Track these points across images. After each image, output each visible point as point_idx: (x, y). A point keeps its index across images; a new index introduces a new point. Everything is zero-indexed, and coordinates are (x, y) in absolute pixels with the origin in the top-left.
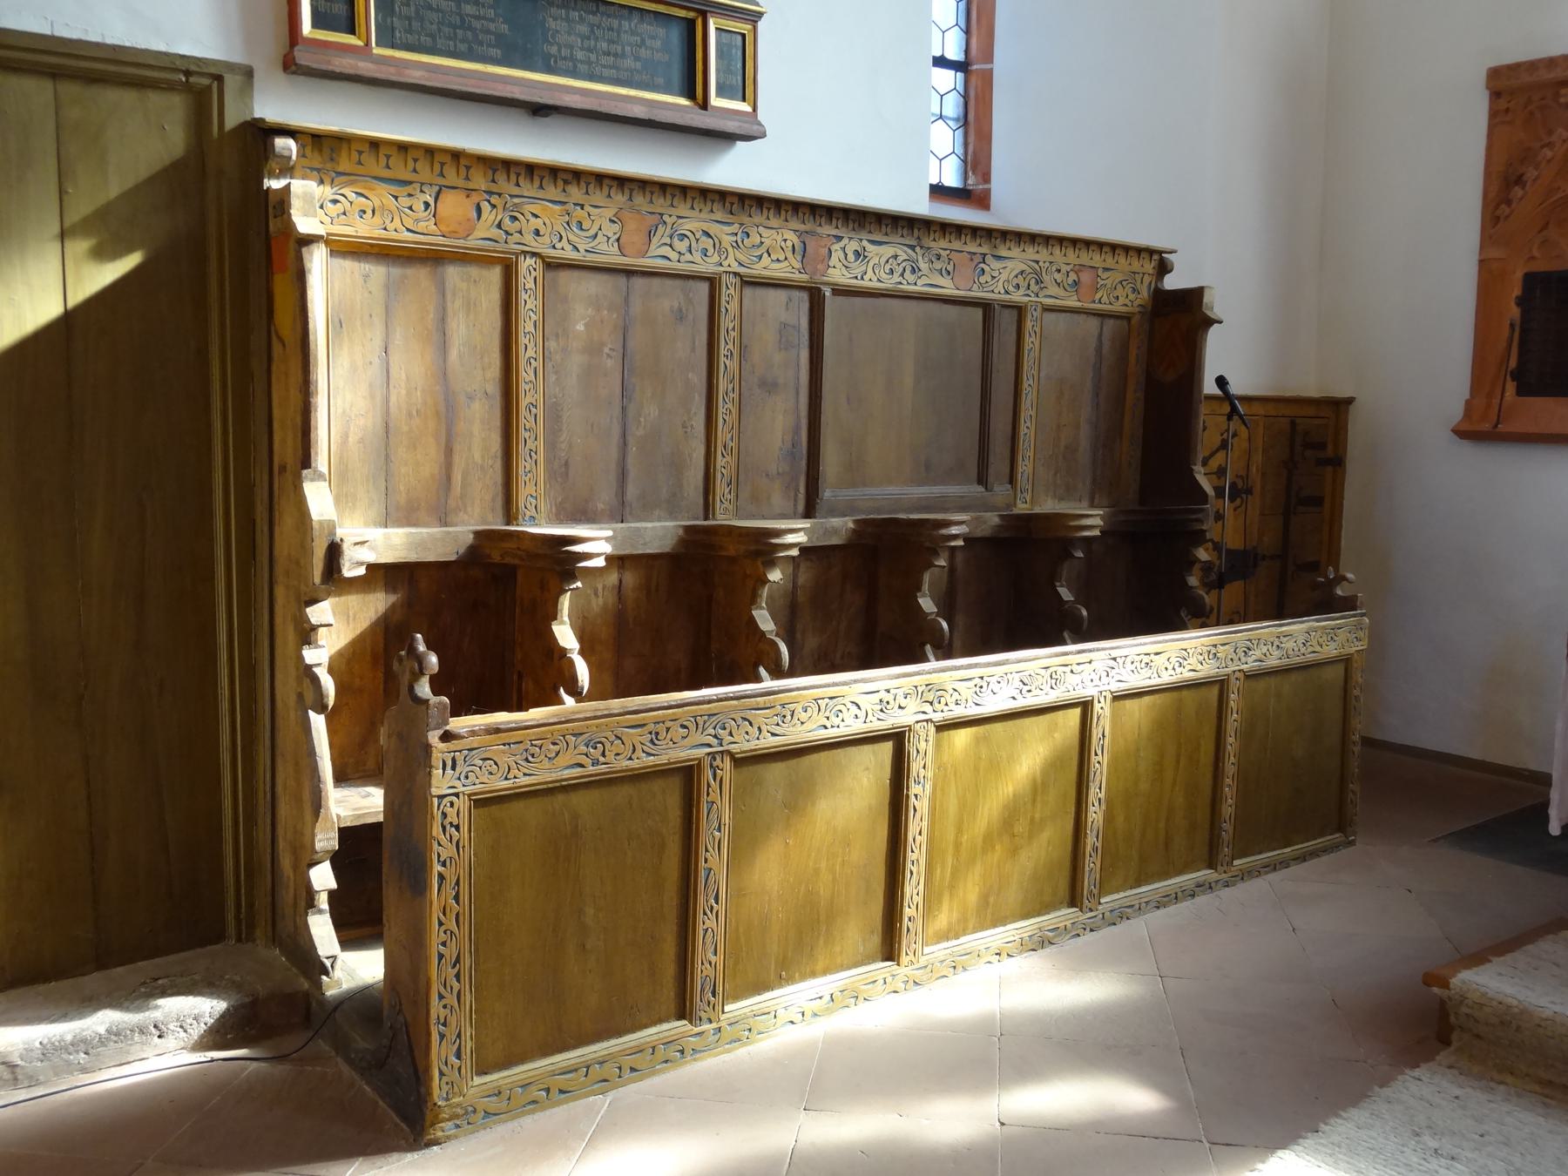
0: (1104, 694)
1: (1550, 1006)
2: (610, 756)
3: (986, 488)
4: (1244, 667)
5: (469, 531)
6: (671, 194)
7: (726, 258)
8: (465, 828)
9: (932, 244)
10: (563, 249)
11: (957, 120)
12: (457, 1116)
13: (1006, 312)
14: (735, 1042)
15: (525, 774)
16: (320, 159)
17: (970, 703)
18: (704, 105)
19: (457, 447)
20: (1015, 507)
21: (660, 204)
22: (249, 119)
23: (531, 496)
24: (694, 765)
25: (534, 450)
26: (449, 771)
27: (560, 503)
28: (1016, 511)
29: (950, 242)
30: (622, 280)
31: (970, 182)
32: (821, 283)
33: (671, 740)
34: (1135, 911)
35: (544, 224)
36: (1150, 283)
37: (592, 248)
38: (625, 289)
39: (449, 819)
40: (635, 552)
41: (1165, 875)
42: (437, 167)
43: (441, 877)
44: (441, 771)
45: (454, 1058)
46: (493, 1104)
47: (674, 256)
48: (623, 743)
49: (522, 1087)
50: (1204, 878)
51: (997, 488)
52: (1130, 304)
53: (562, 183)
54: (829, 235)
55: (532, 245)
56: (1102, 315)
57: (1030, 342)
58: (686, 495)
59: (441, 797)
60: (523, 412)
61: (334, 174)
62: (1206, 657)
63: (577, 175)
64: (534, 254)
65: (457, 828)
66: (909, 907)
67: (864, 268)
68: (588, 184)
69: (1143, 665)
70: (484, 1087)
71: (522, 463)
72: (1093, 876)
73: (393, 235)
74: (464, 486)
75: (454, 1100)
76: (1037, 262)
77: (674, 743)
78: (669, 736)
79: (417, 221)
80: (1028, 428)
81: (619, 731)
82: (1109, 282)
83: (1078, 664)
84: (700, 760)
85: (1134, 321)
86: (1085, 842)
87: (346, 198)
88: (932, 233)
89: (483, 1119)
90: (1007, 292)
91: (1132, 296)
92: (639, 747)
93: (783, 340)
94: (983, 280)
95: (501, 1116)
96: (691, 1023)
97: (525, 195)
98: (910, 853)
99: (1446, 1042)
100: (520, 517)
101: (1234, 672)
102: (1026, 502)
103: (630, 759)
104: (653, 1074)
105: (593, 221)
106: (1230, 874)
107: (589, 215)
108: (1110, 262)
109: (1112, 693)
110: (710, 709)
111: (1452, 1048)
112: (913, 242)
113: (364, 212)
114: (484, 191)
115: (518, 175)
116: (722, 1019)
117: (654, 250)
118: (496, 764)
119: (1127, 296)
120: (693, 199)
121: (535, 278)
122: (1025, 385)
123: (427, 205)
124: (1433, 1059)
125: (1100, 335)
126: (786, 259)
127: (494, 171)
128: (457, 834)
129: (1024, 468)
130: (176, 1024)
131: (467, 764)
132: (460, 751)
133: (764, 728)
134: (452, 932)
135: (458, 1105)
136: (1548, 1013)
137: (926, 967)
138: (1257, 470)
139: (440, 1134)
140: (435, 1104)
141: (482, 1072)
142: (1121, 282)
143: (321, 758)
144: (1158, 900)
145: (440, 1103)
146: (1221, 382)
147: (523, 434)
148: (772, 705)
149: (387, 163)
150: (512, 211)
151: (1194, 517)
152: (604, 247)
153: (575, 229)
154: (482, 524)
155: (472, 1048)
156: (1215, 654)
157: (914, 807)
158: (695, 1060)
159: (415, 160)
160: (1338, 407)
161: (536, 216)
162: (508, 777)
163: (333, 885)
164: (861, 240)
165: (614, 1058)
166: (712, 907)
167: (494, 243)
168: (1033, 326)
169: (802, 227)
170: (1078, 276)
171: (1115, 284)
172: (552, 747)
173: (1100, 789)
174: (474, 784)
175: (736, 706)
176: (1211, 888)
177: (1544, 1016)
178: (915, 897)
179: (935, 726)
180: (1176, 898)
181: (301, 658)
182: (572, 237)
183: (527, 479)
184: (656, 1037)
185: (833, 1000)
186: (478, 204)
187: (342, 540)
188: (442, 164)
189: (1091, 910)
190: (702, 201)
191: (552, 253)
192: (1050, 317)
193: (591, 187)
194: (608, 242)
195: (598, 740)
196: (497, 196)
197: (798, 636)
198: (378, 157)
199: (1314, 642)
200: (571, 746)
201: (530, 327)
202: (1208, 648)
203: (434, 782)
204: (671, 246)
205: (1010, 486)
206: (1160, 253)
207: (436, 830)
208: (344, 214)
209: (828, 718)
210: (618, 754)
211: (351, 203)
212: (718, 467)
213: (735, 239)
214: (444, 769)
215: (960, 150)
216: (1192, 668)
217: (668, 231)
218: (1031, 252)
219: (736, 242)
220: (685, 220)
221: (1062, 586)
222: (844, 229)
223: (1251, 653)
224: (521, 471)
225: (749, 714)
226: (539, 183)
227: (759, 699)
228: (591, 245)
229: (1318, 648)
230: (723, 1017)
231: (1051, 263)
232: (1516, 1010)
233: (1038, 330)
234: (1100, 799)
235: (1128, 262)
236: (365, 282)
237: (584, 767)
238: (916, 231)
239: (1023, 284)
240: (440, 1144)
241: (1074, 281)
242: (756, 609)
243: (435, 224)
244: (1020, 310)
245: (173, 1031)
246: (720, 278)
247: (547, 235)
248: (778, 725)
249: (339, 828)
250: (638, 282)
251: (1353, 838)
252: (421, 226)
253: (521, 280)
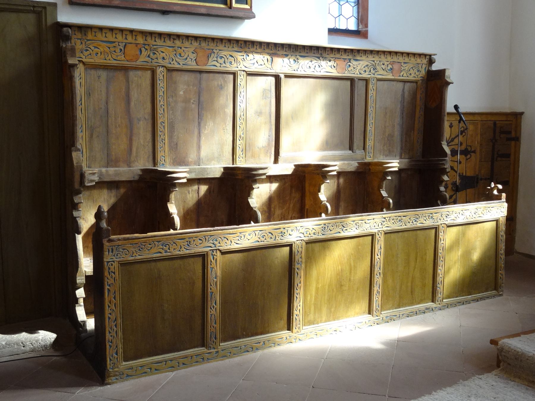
0: (380, 231)
1: (532, 352)
2: (172, 250)
3: (353, 152)
4: (446, 222)
5: (138, 169)
6: (216, 42)
7: (240, 65)
8: (117, 273)
9: (327, 56)
10: (174, 64)
11: (355, 2)
12: (116, 375)
13: (361, 82)
14: (224, 357)
15: (139, 255)
16: (81, 35)
17: (320, 234)
18: (231, 7)
19: (134, 138)
20: (366, 159)
21: (212, 45)
22: (55, 22)
23: (163, 156)
24: (205, 254)
25: (164, 139)
26: (111, 253)
27: (174, 159)
28: (366, 161)
29: (335, 54)
30: (198, 75)
31: (360, 27)
32: (280, 73)
33: (196, 245)
34: (397, 318)
35: (166, 55)
36: (426, 67)
37: (185, 63)
38: (199, 78)
39: (111, 270)
40: (203, 177)
41: (412, 304)
42: (124, 36)
43: (109, 290)
44: (107, 253)
45: (115, 355)
46: (130, 372)
47: (218, 65)
48: (177, 245)
49: (141, 367)
50: (429, 306)
51: (358, 152)
52: (416, 76)
53: (173, 40)
54: (282, 54)
55: (162, 63)
56: (404, 82)
57: (371, 93)
58: (224, 155)
59: (108, 262)
60: (159, 125)
61: (86, 40)
62: (428, 218)
63: (178, 36)
64: (163, 66)
65: (114, 273)
66: (296, 311)
67: (298, 66)
68: (183, 39)
69: (398, 221)
70: (127, 366)
71: (159, 144)
72: (377, 303)
73: (109, 62)
74: (137, 153)
75: (115, 369)
76: (374, 61)
77: (197, 246)
78: (194, 243)
79: (117, 56)
80: (371, 127)
81: (175, 241)
82: (407, 68)
83: (368, 220)
84: (207, 252)
85: (418, 83)
86: (373, 289)
87: (91, 49)
88: (327, 51)
89: (126, 377)
90: (360, 74)
91: (417, 73)
92: (183, 246)
93: (264, 95)
94: (349, 69)
95: (133, 376)
96: (206, 348)
97: (158, 44)
98: (296, 290)
99: (498, 366)
100: (158, 164)
101: (441, 224)
102: (371, 157)
103: (180, 251)
104: (191, 366)
105: (185, 53)
106: (442, 305)
107: (184, 51)
108: (407, 60)
109: (384, 231)
110: (210, 233)
111: (500, 369)
112: (319, 56)
113: (98, 54)
114: (143, 44)
115: (155, 37)
116: (219, 348)
117: (210, 63)
118: (128, 251)
119: (415, 73)
120: (225, 43)
121: (163, 75)
122: (369, 110)
123: (121, 50)
124: (491, 372)
125: (404, 89)
126: (264, 64)
127: (146, 36)
128: (114, 275)
129: (370, 143)
130: (29, 343)
131: (117, 251)
132: (115, 246)
133: (233, 241)
134: (113, 310)
135: (116, 371)
136: (531, 354)
137: (304, 334)
138: (478, 143)
139: (110, 381)
140: (109, 370)
141: (126, 360)
142: (412, 68)
143: (79, 250)
144: (408, 313)
145: (110, 370)
146: (456, 107)
147: (159, 133)
148: (236, 233)
149: (106, 35)
150: (154, 51)
151: (441, 163)
152: (190, 63)
153: (178, 56)
154: (143, 167)
155: (122, 352)
156: (432, 217)
157: (297, 272)
158: (208, 362)
159: (116, 34)
160: (517, 116)
161: (163, 52)
162: (133, 256)
163: (84, 296)
164: (296, 56)
165: (176, 359)
166: (214, 306)
167: (147, 63)
168: (373, 87)
169: (271, 52)
170: (393, 67)
171: (409, 69)
172: (149, 246)
173: (380, 269)
174: (120, 258)
175: (221, 233)
176: (433, 310)
177: (530, 355)
178: (298, 307)
179: (305, 242)
180: (416, 313)
181: (73, 215)
182: (177, 60)
183: (161, 150)
184: (192, 353)
185: (265, 344)
187: (85, 172)
188: (126, 35)
189: (377, 316)
190: (229, 43)
191: (170, 66)
192: (380, 83)
193: (184, 40)
194: (191, 60)
195: (167, 244)
196: (147, 46)
197: (272, 209)
198: (102, 33)
199: (480, 213)
200: (157, 245)
201: (161, 94)
202: (429, 215)
203: (105, 256)
204: (217, 61)
205: (363, 151)
206: (430, 56)
207: (106, 274)
208: (90, 54)
209: (259, 238)
210: (174, 249)
211: (93, 50)
212: (237, 145)
213: (243, 57)
214: (109, 252)
215: (356, 15)
216: (420, 222)
217: (216, 55)
218: (371, 57)
219: (244, 58)
220: (222, 51)
221: (383, 190)
222: (289, 52)
223: (449, 217)
224: (159, 147)
225: (227, 236)
226: (163, 40)
227: (230, 230)
228: (185, 62)
229: (481, 215)
230: (219, 347)
231: (380, 61)
232: (520, 353)
233: (375, 88)
234: (380, 273)
235: (415, 60)
236: (99, 79)
237: (162, 253)
238: (320, 51)
239: (368, 70)
240: (111, 384)
241: (391, 68)
242: (250, 198)
243: (124, 57)
244: (366, 81)
245: (28, 345)
246: (237, 72)
247: (167, 59)
248: (239, 240)
249: (85, 275)
250: (205, 76)
251: (502, 293)
252: (119, 58)
253: (158, 76)
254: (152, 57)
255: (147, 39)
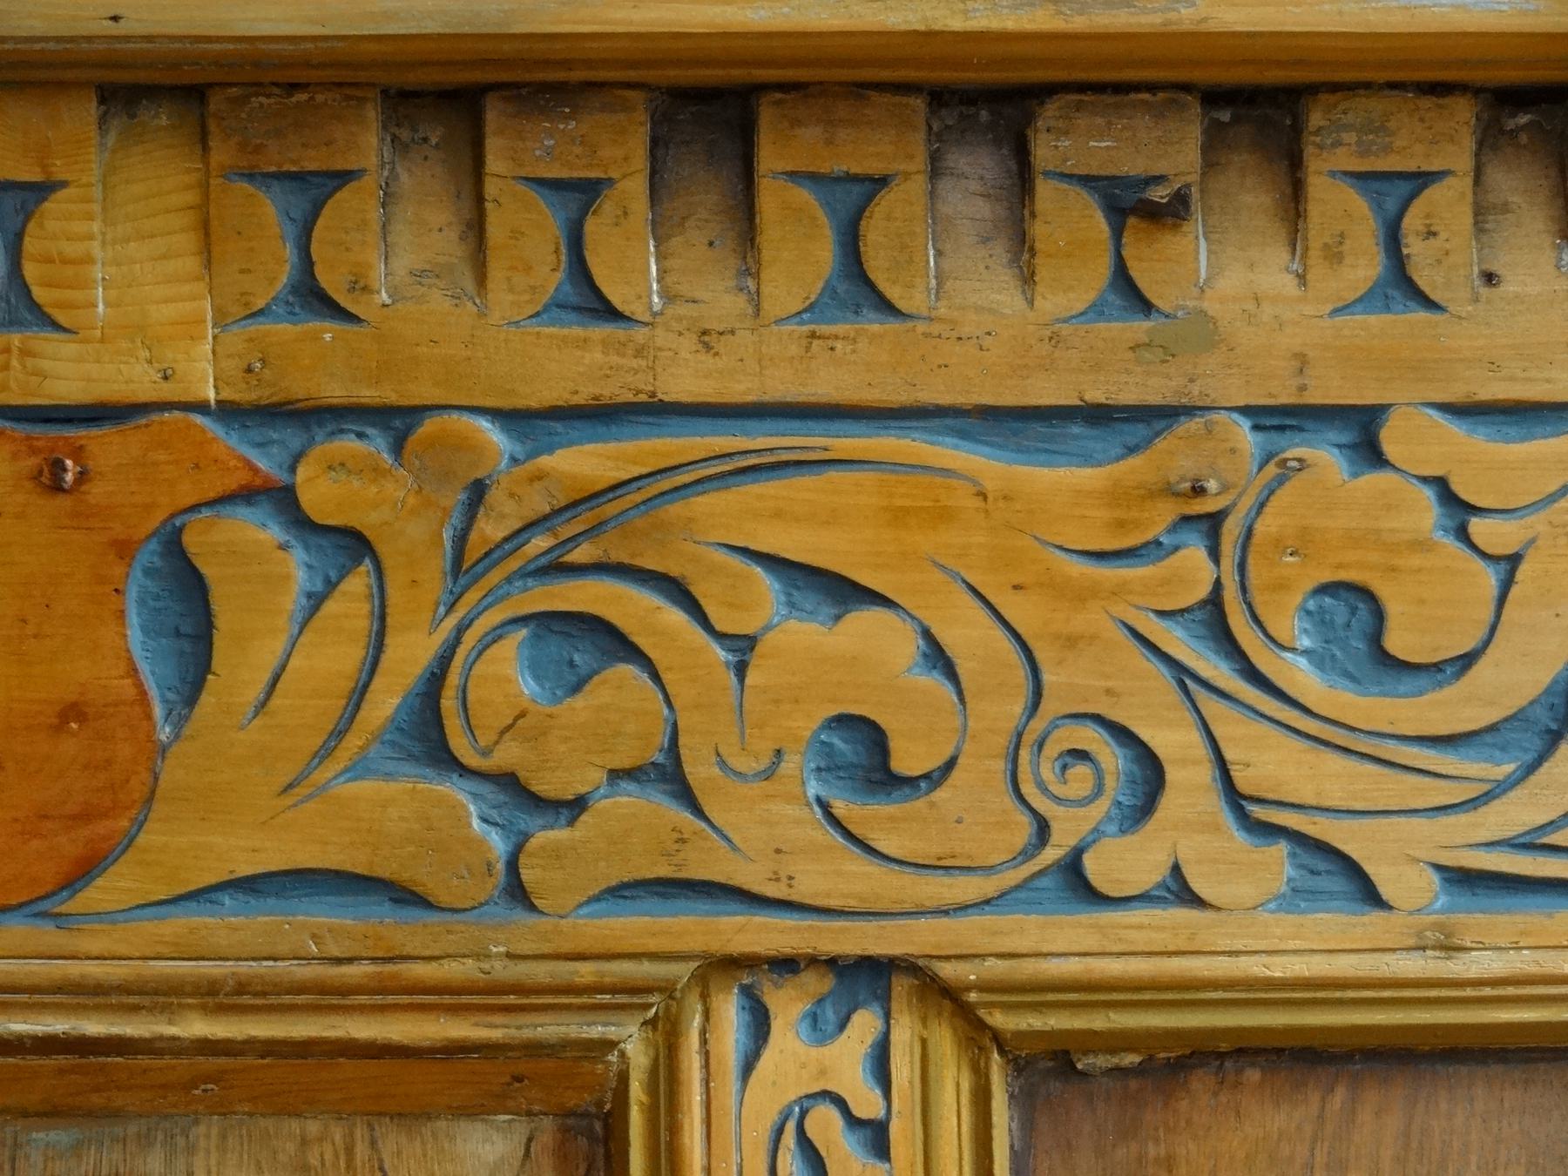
53: (1100, 225)
55: (807, 888)
97: (681, 386)
150: (555, 568)
153: (1299, 675)
186: (174, 546)
196: (376, 445)
226: (825, 253)
254: (507, 755)
255: (331, 281)
